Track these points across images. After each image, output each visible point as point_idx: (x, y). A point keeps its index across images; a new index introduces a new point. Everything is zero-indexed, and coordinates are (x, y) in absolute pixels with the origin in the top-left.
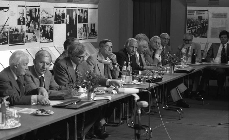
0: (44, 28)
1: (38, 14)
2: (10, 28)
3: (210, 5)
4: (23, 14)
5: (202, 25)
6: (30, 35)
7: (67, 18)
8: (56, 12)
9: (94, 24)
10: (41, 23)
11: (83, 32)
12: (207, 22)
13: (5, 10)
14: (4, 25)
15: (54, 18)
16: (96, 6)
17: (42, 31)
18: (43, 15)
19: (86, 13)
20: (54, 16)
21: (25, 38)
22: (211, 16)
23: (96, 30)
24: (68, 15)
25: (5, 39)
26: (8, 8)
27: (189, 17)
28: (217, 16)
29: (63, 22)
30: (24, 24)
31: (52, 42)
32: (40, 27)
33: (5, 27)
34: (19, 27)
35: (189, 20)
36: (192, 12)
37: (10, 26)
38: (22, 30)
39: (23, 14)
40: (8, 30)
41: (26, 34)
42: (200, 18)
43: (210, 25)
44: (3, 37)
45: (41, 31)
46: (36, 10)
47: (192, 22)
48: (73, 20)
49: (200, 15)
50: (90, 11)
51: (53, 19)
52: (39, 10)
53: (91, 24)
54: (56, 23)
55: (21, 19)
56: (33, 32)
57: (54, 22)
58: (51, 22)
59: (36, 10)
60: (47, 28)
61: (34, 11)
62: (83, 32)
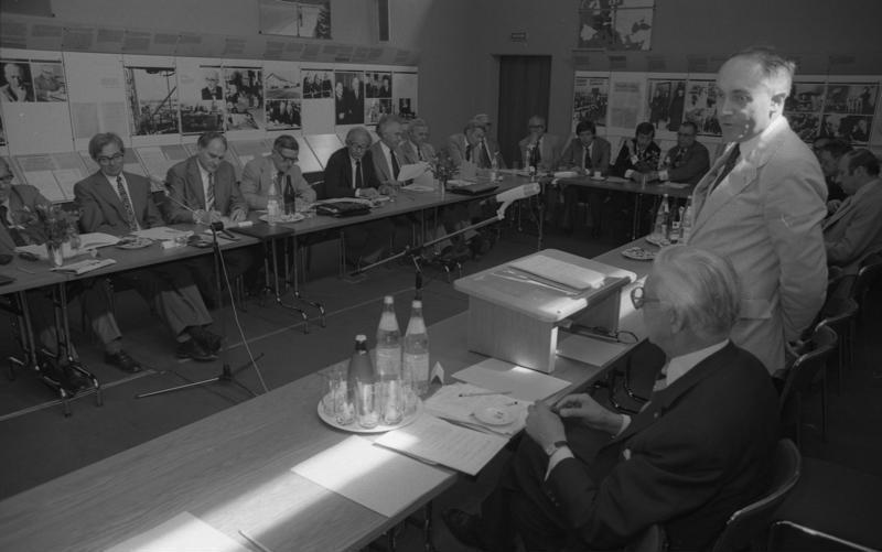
0: (275, 105)
2: (182, 106)
3: (612, 69)
4: (215, 80)
6: (238, 119)
7: (338, 89)
8: (306, 79)
9: (408, 101)
10: (268, 97)
11: (381, 111)
12: (605, 100)
13: (164, 73)
14: (163, 99)
15: (301, 87)
16: (415, 69)
17: (272, 110)
18: (268, 83)
19: (386, 82)
20: (302, 85)
21: (226, 122)
22: (612, 85)
23: (414, 107)
24: (340, 84)
25: (171, 124)
26: (172, 70)
27: (578, 89)
28: (621, 87)
29: (327, 95)
30: (219, 97)
32: (265, 103)
33: (167, 103)
34: (207, 104)
35: (578, 94)
36: (582, 80)
37: (180, 102)
38: (214, 108)
39: (215, 80)
40: (175, 108)
41: (226, 115)
42: (596, 92)
43: (610, 104)
44: (164, 121)
45: (267, 110)
46: (251, 74)
47: (583, 99)
48: (353, 92)
49: (595, 87)
50: (395, 78)
51: (300, 90)
52: (259, 74)
53: (401, 100)
54: (305, 97)
55: (210, 89)
56: (245, 112)
57: (302, 95)
58: (295, 95)
59: (251, 74)
60: (282, 106)
61: (245, 75)
62: (381, 111)
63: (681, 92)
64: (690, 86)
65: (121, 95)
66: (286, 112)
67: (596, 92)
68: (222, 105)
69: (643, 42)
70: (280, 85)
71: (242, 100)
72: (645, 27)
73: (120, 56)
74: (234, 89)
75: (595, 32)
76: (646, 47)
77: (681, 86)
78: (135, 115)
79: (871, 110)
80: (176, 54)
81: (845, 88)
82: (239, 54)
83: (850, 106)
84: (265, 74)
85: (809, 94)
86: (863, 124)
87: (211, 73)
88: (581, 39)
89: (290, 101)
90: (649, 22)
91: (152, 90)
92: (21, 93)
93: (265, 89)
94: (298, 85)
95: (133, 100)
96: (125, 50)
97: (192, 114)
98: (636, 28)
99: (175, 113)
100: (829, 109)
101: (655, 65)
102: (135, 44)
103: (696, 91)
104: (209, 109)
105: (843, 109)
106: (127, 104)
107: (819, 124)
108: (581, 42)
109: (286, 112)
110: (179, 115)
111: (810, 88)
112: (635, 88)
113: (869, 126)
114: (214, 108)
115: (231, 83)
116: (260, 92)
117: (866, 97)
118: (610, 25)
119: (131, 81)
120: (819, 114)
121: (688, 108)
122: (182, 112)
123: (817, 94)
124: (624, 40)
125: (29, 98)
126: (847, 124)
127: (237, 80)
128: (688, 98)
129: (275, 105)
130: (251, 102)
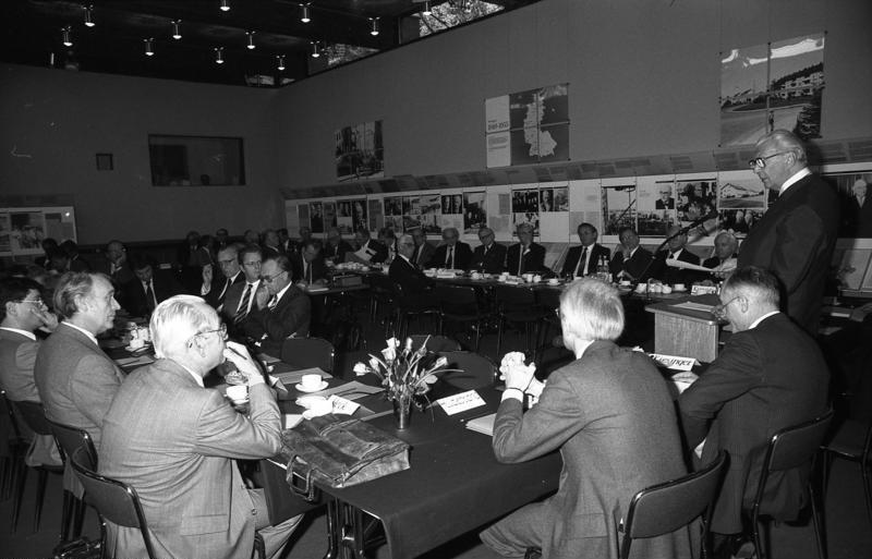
0: (731, 215)
1: (710, 190)
15: (766, 196)
17: (725, 219)
18: (722, 194)
30: (671, 207)
34: (660, 213)
37: (639, 210)
38: (666, 216)
52: (714, 185)
60: (739, 215)
61: (698, 187)
65: (597, 207)
66: (743, 220)
68: (673, 214)
70: (737, 194)
71: (692, 209)
73: (599, 180)
74: (685, 200)
78: (606, 220)
80: (636, 174)
82: (689, 168)
84: (720, 184)
87: (664, 187)
89: (749, 209)
91: (618, 202)
92: (548, 206)
93: (719, 198)
94: (762, 193)
95: (605, 209)
96: (602, 176)
97: (647, 221)
99: (634, 219)
102: (604, 170)
104: (661, 217)
106: (601, 213)
109: (743, 220)
110: (636, 222)
114: (666, 216)
115: (683, 194)
116: (713, 202)
119: (605, 197)
122: (639, 219)
125: (551, 210)
127: (689, 191)
129: (731, 215)
130: (703, 211)
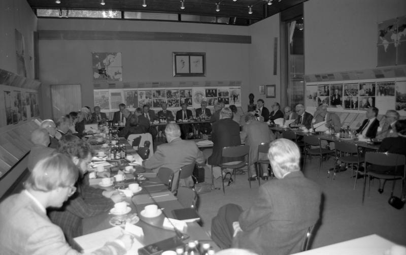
5: (105, 101)
12: (108, 100)
22: (110, 94)
28: (113, 94)
31: (26, 120)
36: (97, 93)
42: (103, 97)
49: (103, 95)
63: (136, 95)
64: (139, 92)
67: (103, 97)
69: (119, 79)
72: (120, 73)
75: (99, 75)
76: (121, 80)
77: (136, 93)
79: (191, 96)
81: (184, 91)
83: (186, 95)
85: (175, 93)
86: (190, 100)
88: (94, 78)
90: (121, 71)
98: (116, 74)
100: (181, 97)
101: (126, 86)
103: (141, 94)
105: (185, 97)
107: (179, 101)
108: (94, 79)
111: (175, 91)
112: (119, 94)
113: (192, 101)
117: (189, 93)
118: (105, 73)
120: (179, 98)
121: (139, 100)
123: (177, 93)
124: (112, 78)
126: (187, 100)
128: (139, 96)
